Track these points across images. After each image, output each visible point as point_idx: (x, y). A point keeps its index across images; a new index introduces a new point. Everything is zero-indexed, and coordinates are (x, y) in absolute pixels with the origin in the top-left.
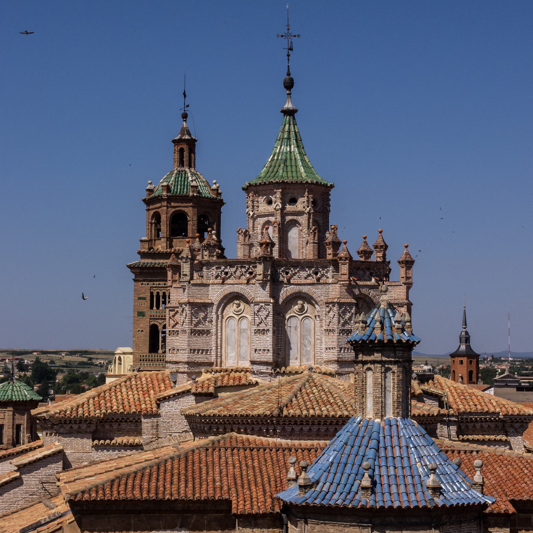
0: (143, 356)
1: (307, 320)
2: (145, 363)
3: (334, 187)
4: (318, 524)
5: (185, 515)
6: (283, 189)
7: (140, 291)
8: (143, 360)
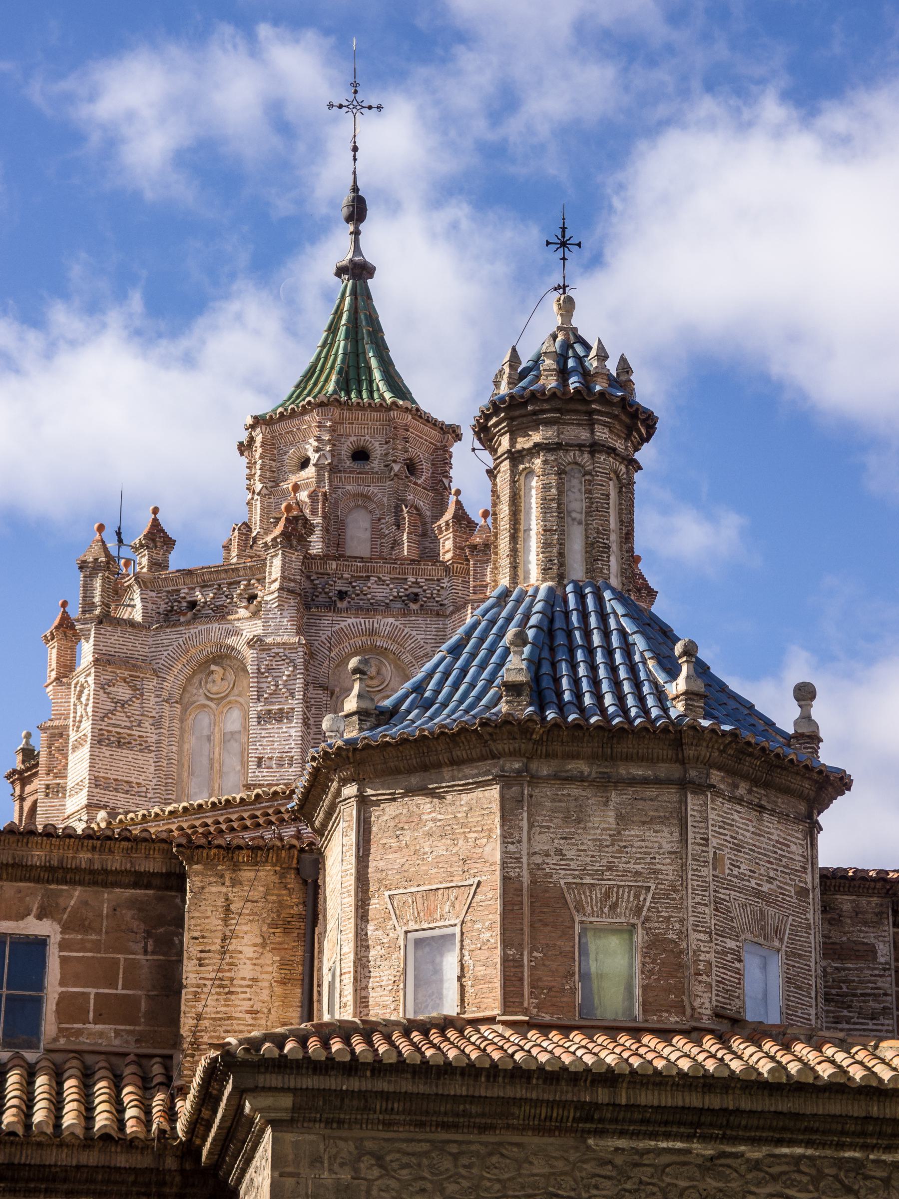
3: (460, 440)
4: (394, 800)
5: (53, 886)
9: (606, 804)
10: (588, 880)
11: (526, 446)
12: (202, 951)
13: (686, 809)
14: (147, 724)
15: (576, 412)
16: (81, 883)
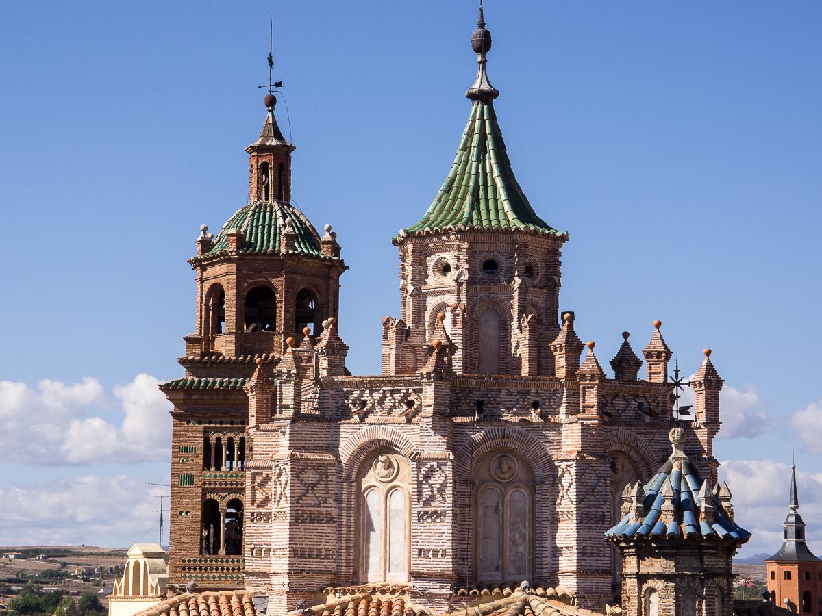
0: (189, 561)
2: (193, 575)
6: (470, 243)
7: (186, 435)
8: (189, 569)
14: (331, 500)
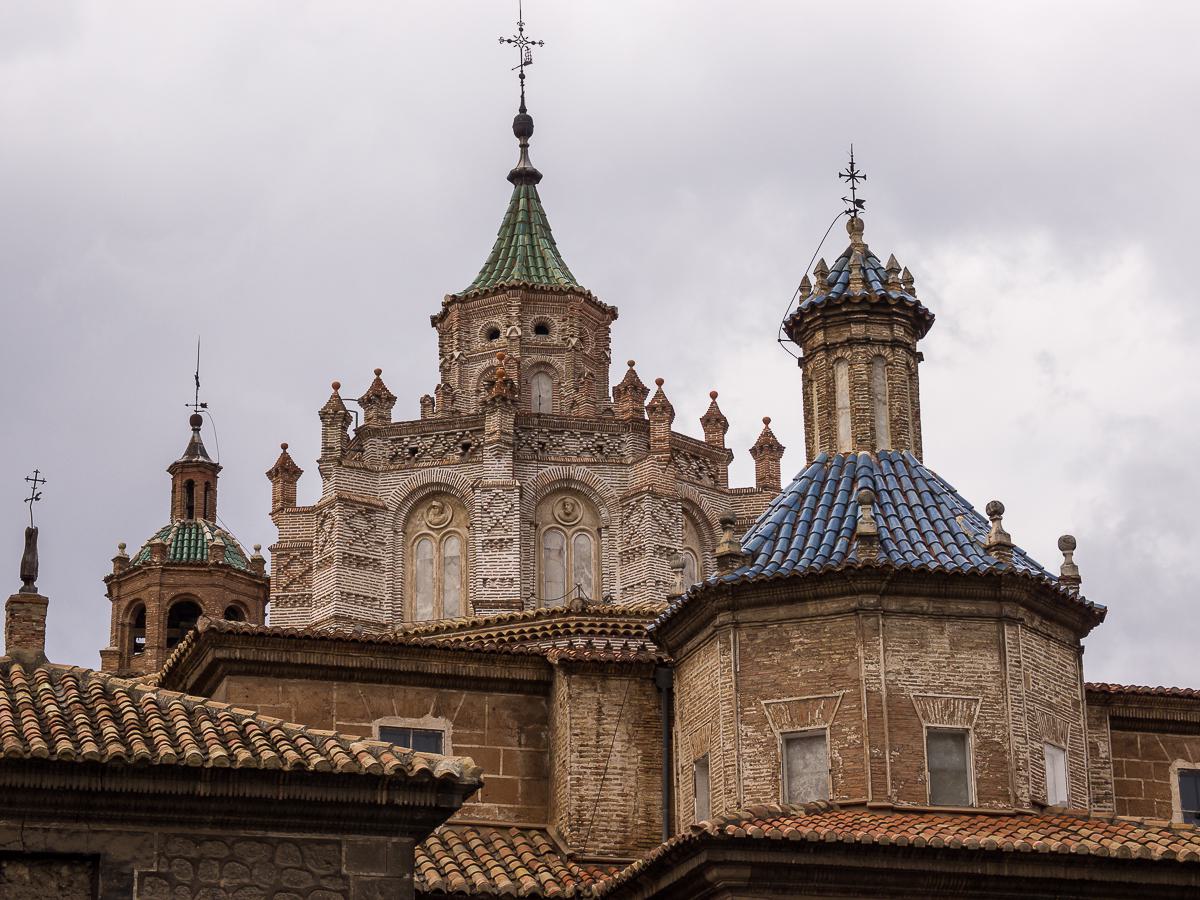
1: (581, 537)
5: (445, 690)
9: (942, 632)
10: (930, 694)
11: (839, 340)
12: (581, 746)
13: (1003, 637)
15: (878, 314)
16: (468, 688)
